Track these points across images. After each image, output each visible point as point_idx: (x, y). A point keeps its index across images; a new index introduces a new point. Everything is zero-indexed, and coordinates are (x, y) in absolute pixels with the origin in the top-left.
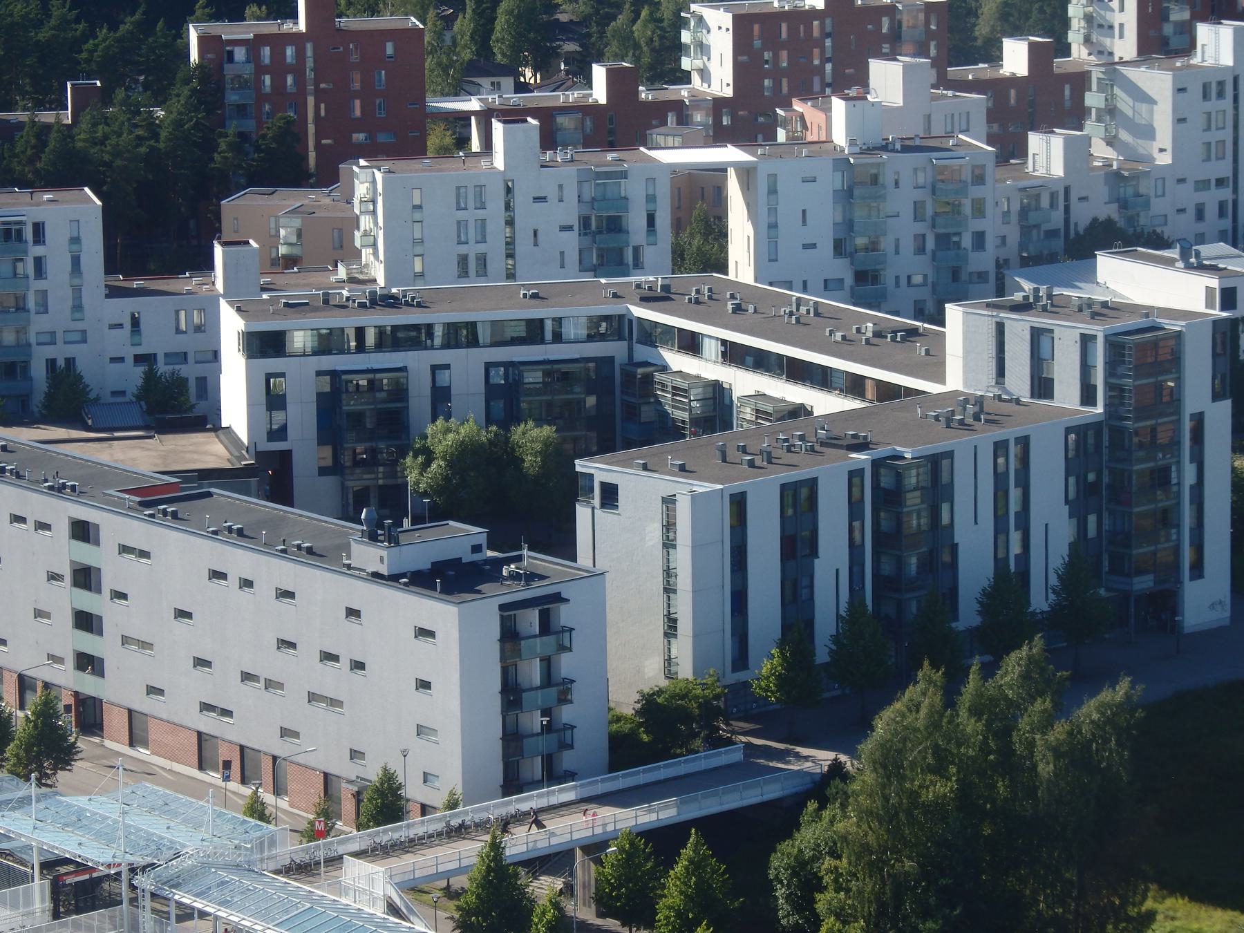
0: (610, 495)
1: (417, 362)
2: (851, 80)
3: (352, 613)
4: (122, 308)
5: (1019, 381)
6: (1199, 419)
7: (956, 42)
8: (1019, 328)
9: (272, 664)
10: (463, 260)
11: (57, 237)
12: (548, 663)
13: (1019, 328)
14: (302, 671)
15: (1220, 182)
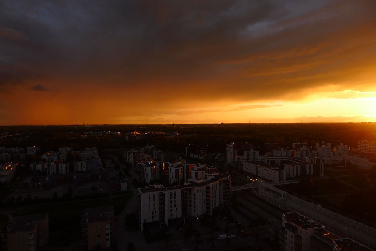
1: (276, 160)
2: (302, 147)
3: (271, 171)
5: (310, 162)
7: (308, 146)
8: (310, 159)
12: (282, 175)
13: (310, 159)
15: (324, 154)
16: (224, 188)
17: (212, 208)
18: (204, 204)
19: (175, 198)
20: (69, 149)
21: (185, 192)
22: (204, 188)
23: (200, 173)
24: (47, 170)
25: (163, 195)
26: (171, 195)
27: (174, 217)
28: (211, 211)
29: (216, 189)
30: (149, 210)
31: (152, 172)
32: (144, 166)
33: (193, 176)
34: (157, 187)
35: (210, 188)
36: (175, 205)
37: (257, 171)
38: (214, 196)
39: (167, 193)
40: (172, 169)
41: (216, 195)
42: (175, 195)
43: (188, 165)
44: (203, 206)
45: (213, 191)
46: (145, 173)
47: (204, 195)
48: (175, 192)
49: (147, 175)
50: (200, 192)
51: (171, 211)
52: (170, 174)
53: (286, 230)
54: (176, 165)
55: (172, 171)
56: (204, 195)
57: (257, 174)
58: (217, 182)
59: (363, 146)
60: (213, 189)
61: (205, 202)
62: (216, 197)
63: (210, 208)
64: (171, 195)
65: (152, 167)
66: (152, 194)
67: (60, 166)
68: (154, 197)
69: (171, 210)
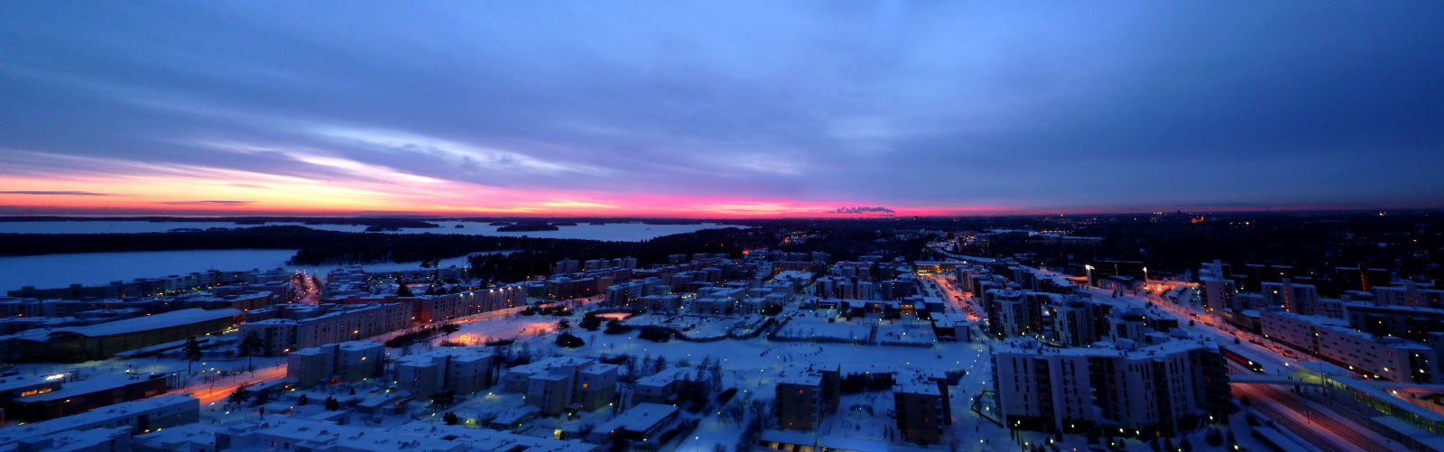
33: (1114, 330)
37: (1315, 342)
46: (1001, 313)
47: (1148, 378)
49: (1005, 317)
57: (1316, 348)
65: (1013, 302)
68: (1025, 365)
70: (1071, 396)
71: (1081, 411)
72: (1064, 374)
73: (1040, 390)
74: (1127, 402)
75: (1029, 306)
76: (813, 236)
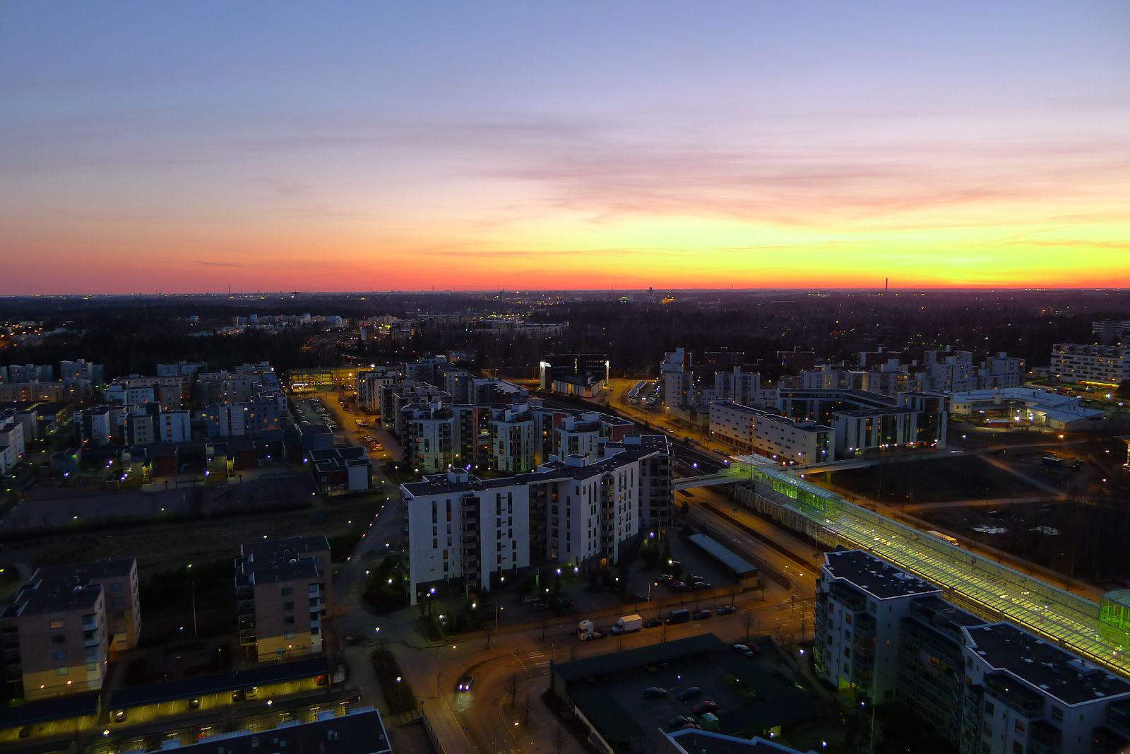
0: (837, 419)
1: (808, 400)
4: (762, 391)
6: (941, 414)
9: (780, 441)
10: (818, 381)
11: (753, 378)
14: (785, 443)
16: (654, 483)
17: (620, 540)
18: (595, 529)
19: (510, 512)
20: (188, 368)
21: (539, 494)
22: (595, 483)
23: (584, 437)
24: (126, 432)
25: (476, 502)
26: (499, 504)
27: (507, 565)
28: (616, 548)
29: (632, 486)
30: (435, 546)
31: (440, 436)
32: (416, 419)
33: (564, 444)
34: (458, 478)
35: (612, 482)
36: (510, 531)
38: (625, 504)
39: (486, 498)
40: (500, 425)
41: (630, 503)
42: (510, 502)
43: (549, 414)
44: (592, 534)
45: (623, 489)
48: (510, 494)
49: (427, 445)
50: (584, 493)
51: (499, 549)
52: (495, 440)
53: (831, 600)
54: (512, 414)
55: (499, 434)
56: (595, 501)
58: (635, 466)
59: (1099, 374)
60: (623, 484)
61: (598, 523)
62: (630, 508)
63: (611, 539)
64: (499, 504)
65: (442, 422)
66: (441, 499)
67: (162, 418)
69: (499, 545)
70: (505, 540)
71: (515, 559)
72: (499, 513)
73: (466, 541)
74: (569, 534)
75: (462, 424)
76: (58, 331)
